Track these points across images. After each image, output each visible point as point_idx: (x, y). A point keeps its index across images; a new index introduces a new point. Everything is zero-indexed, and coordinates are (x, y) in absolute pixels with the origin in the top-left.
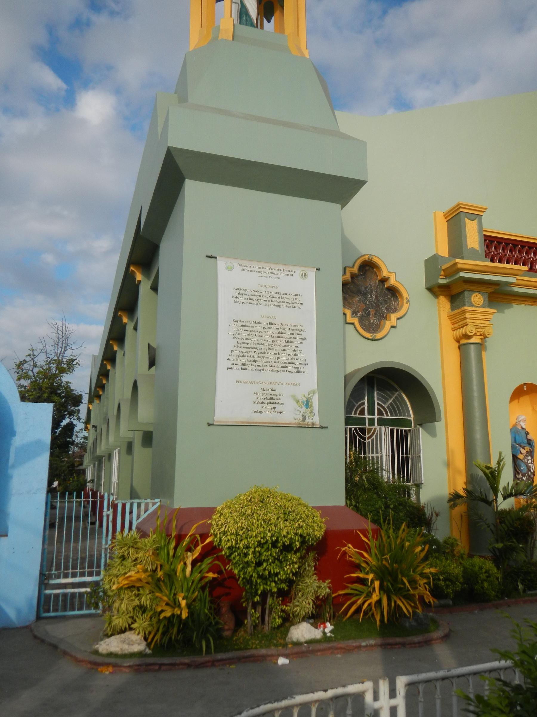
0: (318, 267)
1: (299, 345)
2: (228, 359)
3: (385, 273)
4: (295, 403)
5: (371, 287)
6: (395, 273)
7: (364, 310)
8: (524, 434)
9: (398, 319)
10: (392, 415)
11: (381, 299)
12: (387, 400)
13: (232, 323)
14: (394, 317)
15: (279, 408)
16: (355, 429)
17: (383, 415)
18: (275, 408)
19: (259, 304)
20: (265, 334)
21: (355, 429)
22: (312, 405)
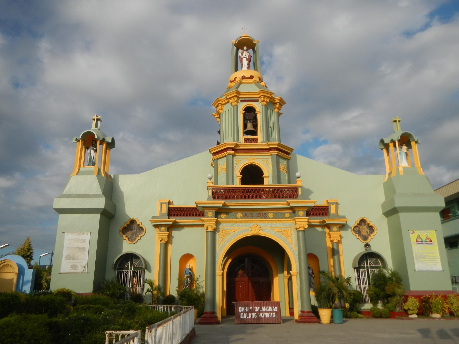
0: (91, 231)
1: (84, 252)
2: (65, 257)
3: (138, 223)
4: (81, 267)
5: (135, 227)
6: (142, 223)
7: (132, 235)
8: (188, 270)
9: (141, 237)
10: (138, 266)
11: (137, 231)
12: (137, 262)
13: (67, 248)
14: (140, 236)
15: (77, 269)
16: (126, 271)
17: (135, 266)
18: (76, 269)
19: (74, 243)
20: (75, 250)
21: (126, 271)
22: (86, 267)
